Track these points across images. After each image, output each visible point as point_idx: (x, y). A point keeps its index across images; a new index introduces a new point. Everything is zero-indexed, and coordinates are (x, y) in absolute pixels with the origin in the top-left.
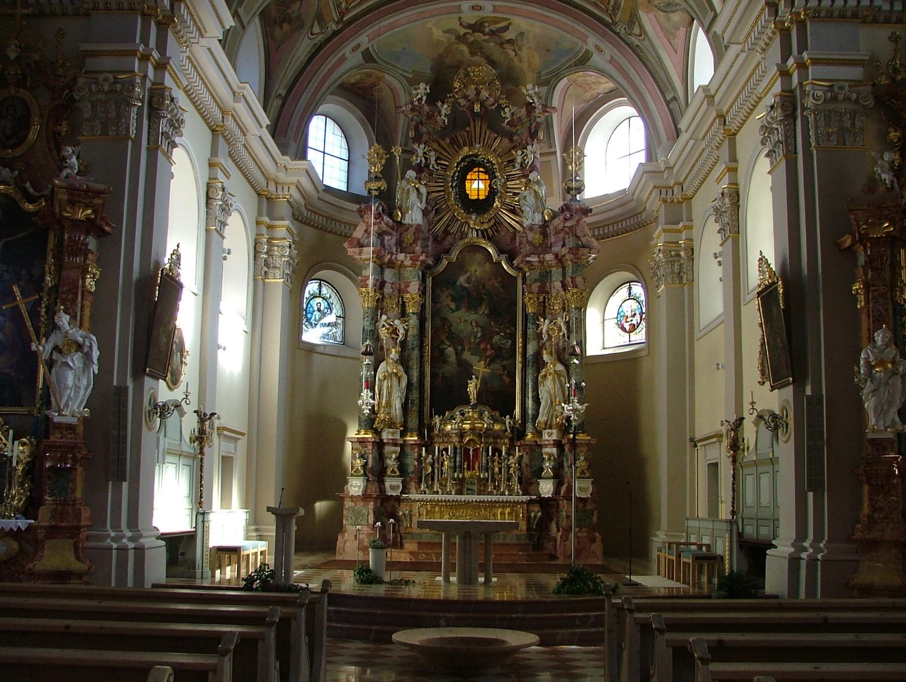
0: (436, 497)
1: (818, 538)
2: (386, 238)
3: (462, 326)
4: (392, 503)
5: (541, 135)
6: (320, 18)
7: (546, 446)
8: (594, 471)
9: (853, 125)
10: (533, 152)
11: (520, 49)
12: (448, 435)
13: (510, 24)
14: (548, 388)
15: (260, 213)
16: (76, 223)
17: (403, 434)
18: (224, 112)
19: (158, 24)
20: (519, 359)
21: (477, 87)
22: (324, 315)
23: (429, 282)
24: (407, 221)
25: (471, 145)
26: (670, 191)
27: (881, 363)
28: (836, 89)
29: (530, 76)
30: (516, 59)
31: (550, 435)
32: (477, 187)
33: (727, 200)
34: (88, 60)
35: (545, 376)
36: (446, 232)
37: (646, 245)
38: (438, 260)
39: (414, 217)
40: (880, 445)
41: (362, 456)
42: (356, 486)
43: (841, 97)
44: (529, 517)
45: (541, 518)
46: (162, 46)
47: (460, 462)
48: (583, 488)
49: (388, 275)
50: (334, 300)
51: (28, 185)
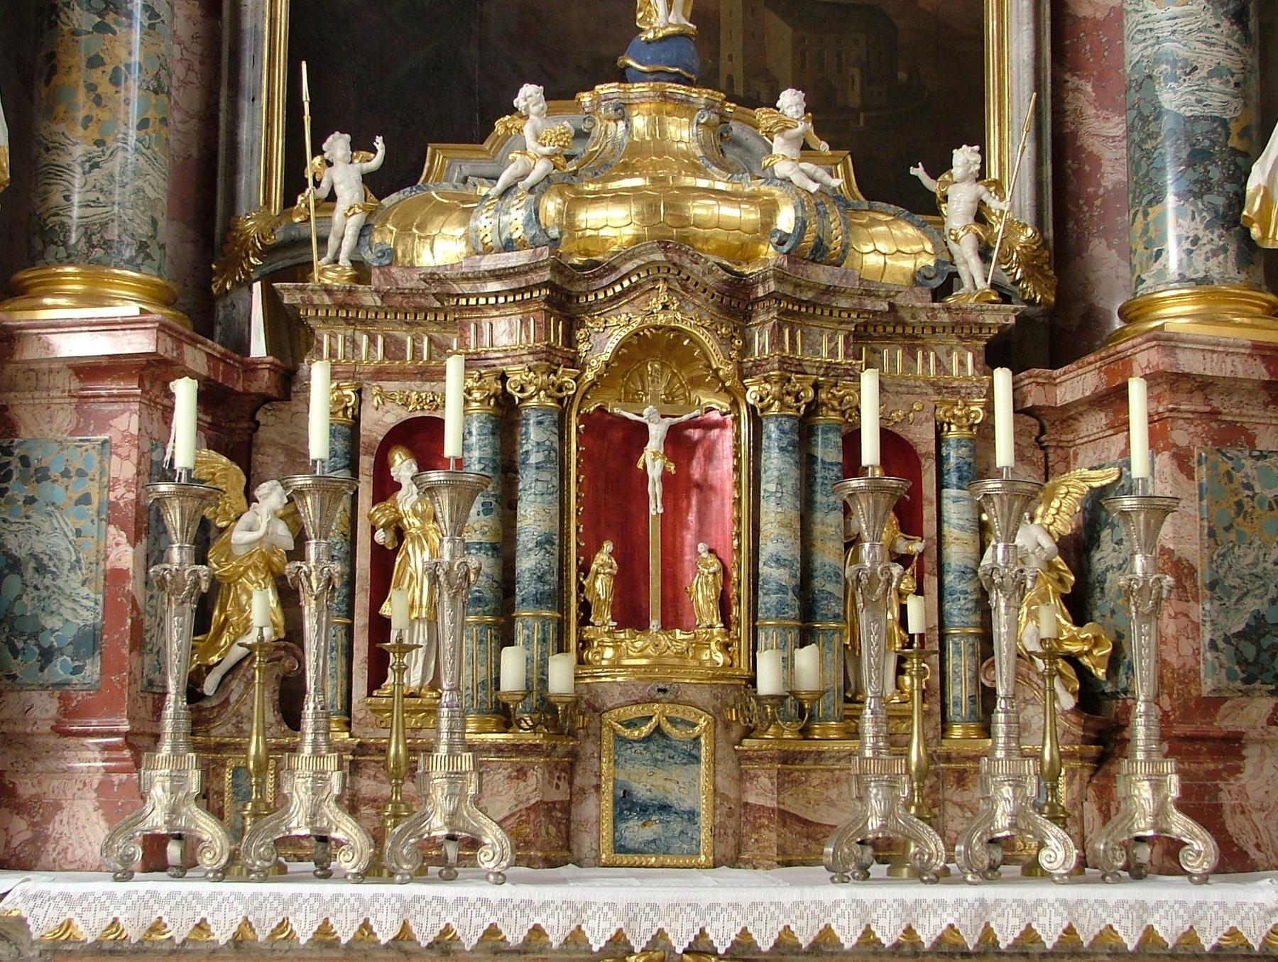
47: (555, 542)
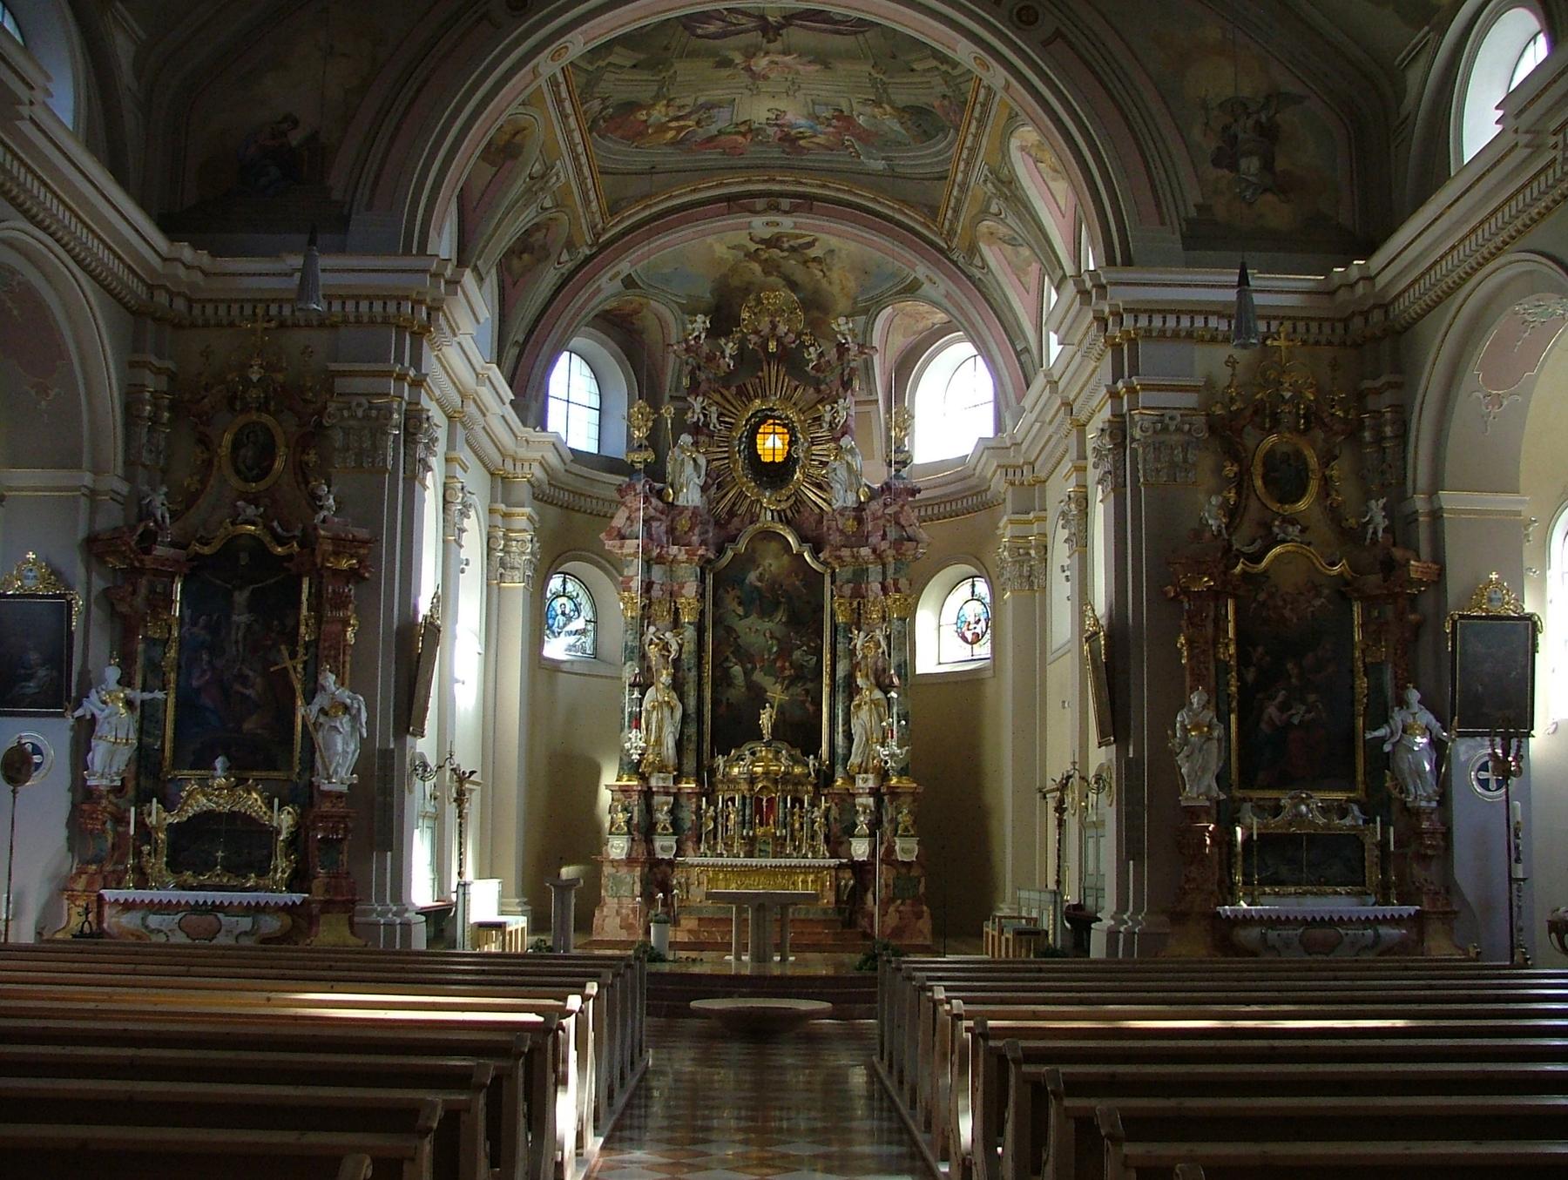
0: (720, 861)
1: (1137, 910)
2: (655, 524)
3: (752, 638)
4: (663, 867)
5: (856, 384)
6: (570, 245)
7: (861, 795)
8: (922, 827)
9: (1185, 460)
10: (846, 408)
11: (830, 269)
12: (734, 781)
13: (815, 240)
14: (862, 720)
15: (493, 500)
16: (336, 573)
17: (677, 780)
18: (463, 397)
19: (413, 333)
20: (826, 680)
21: (772, 317)
22: (570, 619)
23: (709, 580)
24: (681, 502)
25: (764, 397)
26: (1018, 472)
27: (1197, 727)
28: (1167, 420)
29: (843, 304)
30: (824, 281)
31: (865, 781)
32: (772, 445)
33: (1073, 506)
34: (337, 380)
35: (859, 706)
36: (731, 513)
37: (991, 535)
38: (720, 551)
39: (690, 496)
40: (1194, 813)
41: (625, 809)
42: (618, 847)
43: (1172, 428)
44: (838, 886)
45: (853, 887)
46: (417, 361)
48: (906, 849)
49: (657, 573)
50: (583, 599)
51: (275, 524)
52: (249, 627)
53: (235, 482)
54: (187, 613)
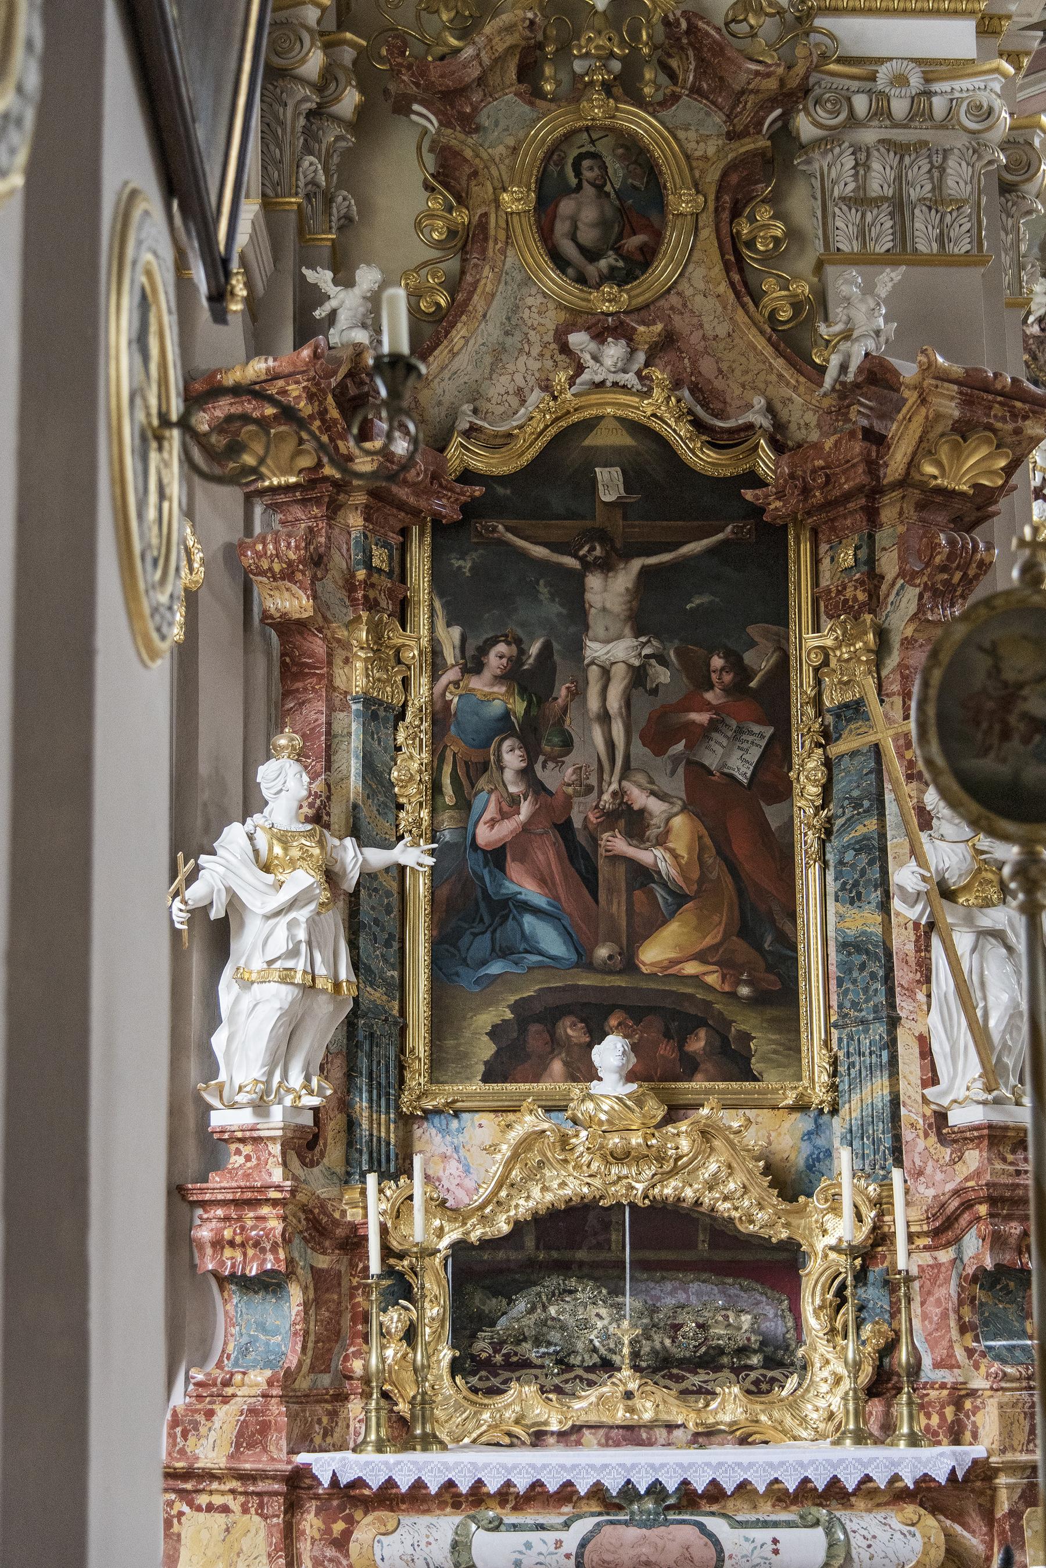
52: (638, 676)
53: (552, 280)
54: (450, 637)
